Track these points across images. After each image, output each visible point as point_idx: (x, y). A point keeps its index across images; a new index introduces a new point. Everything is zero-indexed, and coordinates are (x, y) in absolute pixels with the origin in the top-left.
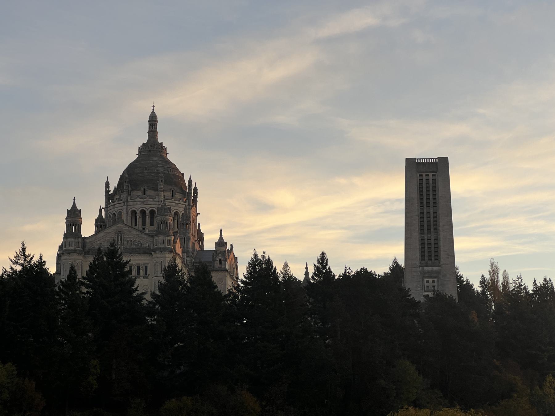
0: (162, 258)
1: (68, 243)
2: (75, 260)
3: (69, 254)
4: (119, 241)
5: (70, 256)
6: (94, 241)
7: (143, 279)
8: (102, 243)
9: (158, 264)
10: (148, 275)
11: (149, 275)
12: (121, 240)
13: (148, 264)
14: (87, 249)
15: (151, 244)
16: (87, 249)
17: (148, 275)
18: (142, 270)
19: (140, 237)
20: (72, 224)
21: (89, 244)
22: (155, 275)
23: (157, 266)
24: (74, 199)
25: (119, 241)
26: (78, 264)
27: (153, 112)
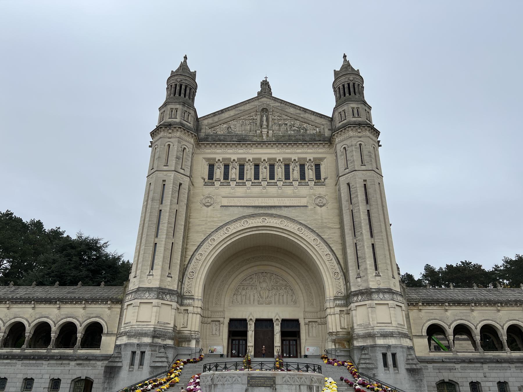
0: (360, 137)
1: (168, 113)
2: (180, 139)
3: (168, 128)
4: (265, 123)
5: (170, 131)
6: (217, 122)
7: (314, 185)
9: (354, 149)
10: (323, 180)
11: (325, 179)
12: (267, 120)
13: (322, 159)
14: (202, 135)
15: (324, 128)
16: (202, 135)
17: (323, 180)
19: (302, 117)
21: (207, 127)
25: (265, 123)
26: (185, 148)
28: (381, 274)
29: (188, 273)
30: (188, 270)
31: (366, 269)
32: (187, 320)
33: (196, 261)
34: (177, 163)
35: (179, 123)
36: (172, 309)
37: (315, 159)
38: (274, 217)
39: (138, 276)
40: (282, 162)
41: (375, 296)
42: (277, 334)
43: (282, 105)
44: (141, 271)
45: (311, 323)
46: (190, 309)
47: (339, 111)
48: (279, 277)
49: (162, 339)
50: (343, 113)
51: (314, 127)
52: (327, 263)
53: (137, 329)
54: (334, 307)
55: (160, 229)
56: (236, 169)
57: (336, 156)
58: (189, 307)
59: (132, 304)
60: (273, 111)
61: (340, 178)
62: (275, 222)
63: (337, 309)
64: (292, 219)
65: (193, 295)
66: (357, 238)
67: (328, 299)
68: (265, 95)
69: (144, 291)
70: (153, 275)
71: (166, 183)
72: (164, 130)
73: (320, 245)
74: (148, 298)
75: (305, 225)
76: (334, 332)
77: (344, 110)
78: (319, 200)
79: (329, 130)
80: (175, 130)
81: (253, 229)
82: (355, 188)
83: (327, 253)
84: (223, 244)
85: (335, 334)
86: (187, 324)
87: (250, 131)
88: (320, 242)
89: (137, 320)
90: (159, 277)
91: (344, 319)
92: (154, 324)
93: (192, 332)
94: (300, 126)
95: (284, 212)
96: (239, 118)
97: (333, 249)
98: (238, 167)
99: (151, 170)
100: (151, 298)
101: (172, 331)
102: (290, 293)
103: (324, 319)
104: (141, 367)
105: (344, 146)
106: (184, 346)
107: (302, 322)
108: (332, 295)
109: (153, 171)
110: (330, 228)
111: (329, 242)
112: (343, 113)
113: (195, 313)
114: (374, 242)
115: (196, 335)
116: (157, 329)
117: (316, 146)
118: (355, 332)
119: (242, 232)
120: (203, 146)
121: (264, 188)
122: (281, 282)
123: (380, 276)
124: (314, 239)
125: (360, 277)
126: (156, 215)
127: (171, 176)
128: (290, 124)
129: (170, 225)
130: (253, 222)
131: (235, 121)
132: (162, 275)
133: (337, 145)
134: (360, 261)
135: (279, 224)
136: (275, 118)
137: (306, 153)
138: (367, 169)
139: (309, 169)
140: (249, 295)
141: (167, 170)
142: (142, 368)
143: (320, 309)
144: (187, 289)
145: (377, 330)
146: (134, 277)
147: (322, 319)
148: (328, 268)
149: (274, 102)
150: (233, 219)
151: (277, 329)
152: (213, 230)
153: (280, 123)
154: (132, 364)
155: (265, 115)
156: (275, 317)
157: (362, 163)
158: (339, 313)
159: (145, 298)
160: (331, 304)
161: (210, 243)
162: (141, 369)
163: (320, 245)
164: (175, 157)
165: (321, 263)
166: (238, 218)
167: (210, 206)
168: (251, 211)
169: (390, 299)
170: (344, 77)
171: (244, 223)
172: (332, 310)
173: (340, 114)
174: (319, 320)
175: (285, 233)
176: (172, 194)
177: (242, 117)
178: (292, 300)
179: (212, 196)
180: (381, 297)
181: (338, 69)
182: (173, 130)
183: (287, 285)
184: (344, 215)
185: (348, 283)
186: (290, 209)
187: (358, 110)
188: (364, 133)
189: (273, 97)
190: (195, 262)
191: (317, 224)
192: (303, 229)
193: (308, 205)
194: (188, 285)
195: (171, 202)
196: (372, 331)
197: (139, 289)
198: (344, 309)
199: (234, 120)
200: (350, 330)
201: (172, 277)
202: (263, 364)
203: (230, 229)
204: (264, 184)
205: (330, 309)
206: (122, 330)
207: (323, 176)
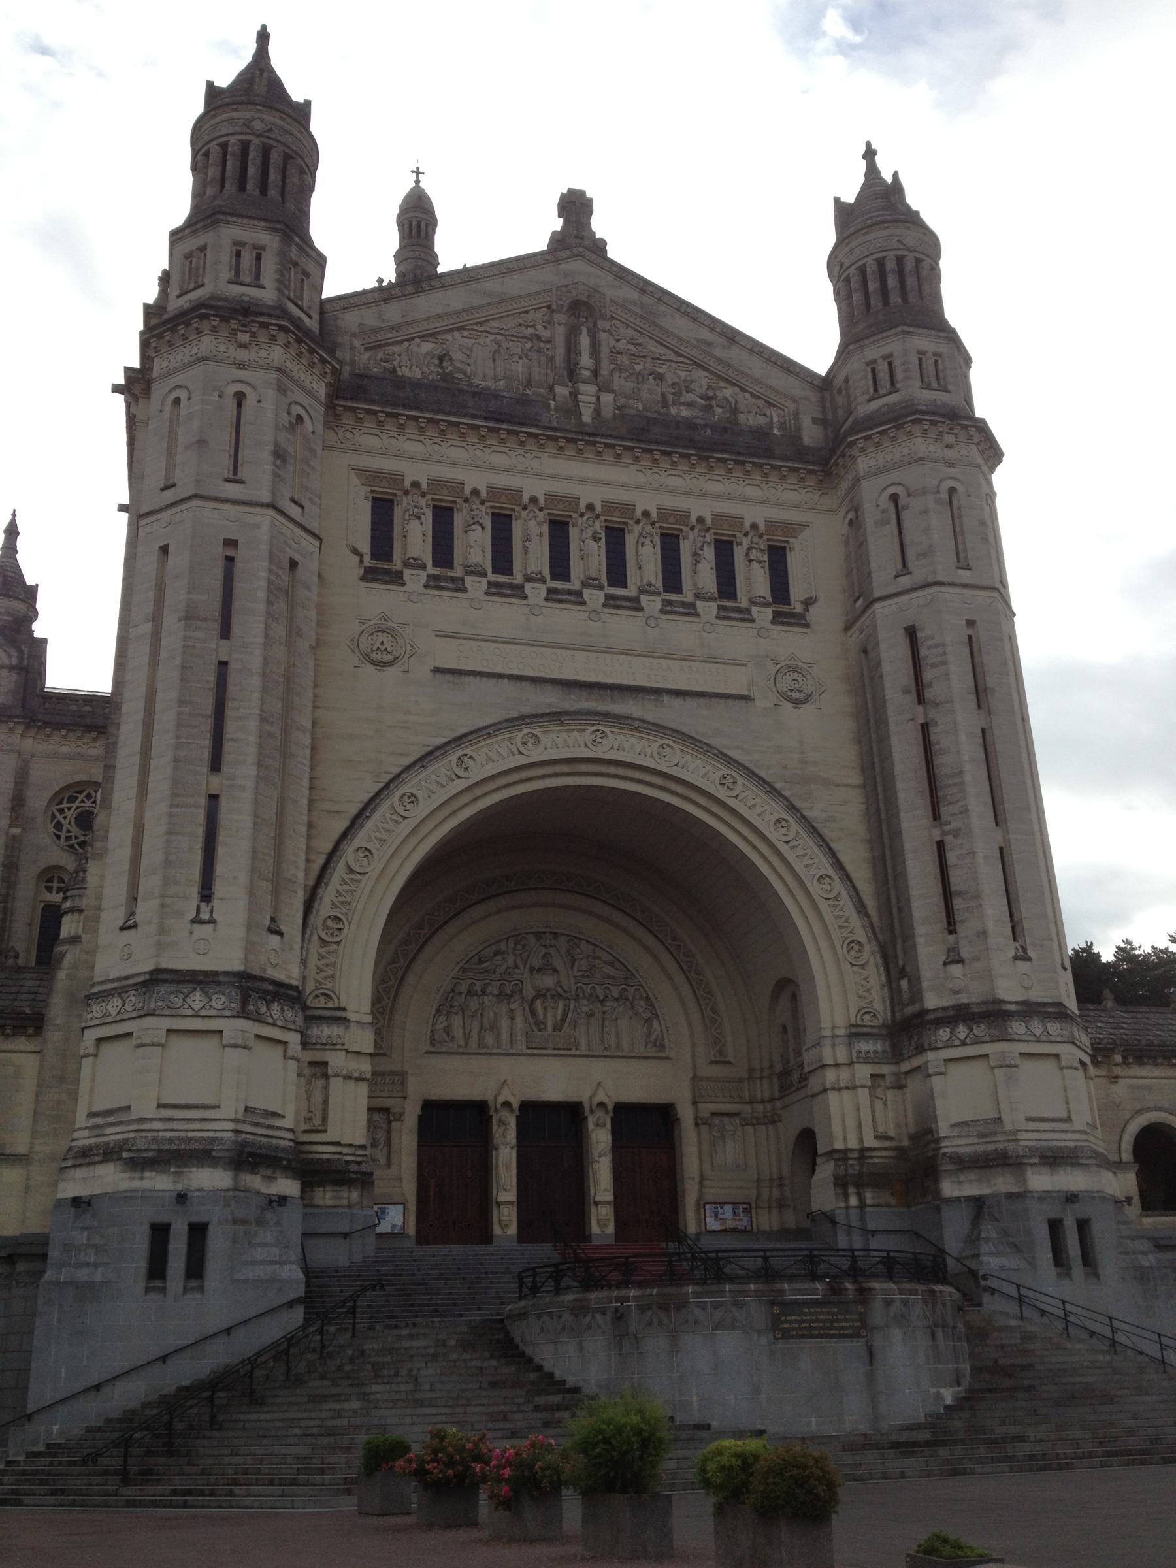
0: (951, 464)
3: (234, 325)
5: (244, 337)
8: (457, 356)
11: (808, 603)
13: (793, 529)
18: (754, 564)
19: (719, 360)
22: (905, 581)
23: (926, 512)
25: (586, 360)
28: (1031, 953)
29: (319, 924)
30: (318, 911)
31: (983, 934)
32: (325, 1102)
33: (346, 877)
34: (279, 476)
35: (272, 307)
36: (285, 1057)
37: (772, 525)
38: (637, 729)
40: (653, 524)
41: (1017, 1027)
42: (603, 1159)
43: (646, 299)
44: (163, 906)
45: (717, 1121)
46: (336, 1061)
47: (870, 358)
48: (599, 953)
49: (264, 1177)
50: (883, 368)
51: (761, 403)
52: (823, 906)
53: (162, 1134)
54: (851, 1064)
55: (232, 739)
56: (483, 528)
57: (855, 524)
58: (328, 1052)
59: (131, 1034)
60: (612, 316)
61: (877, 606)
62: (638, 748)
63: (863, 1072)
64: (701, 742)
65: (342, 1005)
66: (949, 823)
67: (827, 1033)
68: (581, 249)
69: (178, 982)
70: (212, 921)
71: (241, 554)
72: (214, 330)
73: (797, 843)
74: (203, 1013)
75: (745, 767)
76: (851, 1150)
77: (890, 355)
78: (789, 678)
79: (815, 420)
80: (263, 336)
81: (559, 769)
82: (937, 646)
83: (823, 872)
84: (445, 819)
85: (856, 1155)
86: (325, 1119)
87: (529, 384)
88: (798, 833)
89: (159, 1099)
90: (241, 933)
91: (885, 1104)
92: (232, 1116)
93: (345, 1150)
94: (711, 393)
95: (671, 713)
96: (482, 323)
97: (843, 858)
98: (487, 522)
99: (163, 490)
100: (212, 1013)
101: (292, 1144)
102: (641, 1010)
103: (768, 1106)
104: (194, 1283)
105: (892, 490)
106: (321, 1203)
107: (686, 1114)
108: (840, 1021)
109: (170, 496)
110: (827, 782)
111: (825, 832)
112: (883, 368)
113: (350, 1078)
114: (1007, 840)
115: (359, 1159)
116: (244, 1136)
117: (774, 478)
118: (943, 1151)
119: (516, 777)
120: (348, 420)
121: (593, 616)
122: (608, 970)
123: (1029, 959)
124: (778, 821)
125: (961, 961)
126: (207, 682)
127: (257, 526)
128: (676, 380)
129: (267, 728)
130: (559, 741)
131: (466, 333)
132: (249, 928)
133: (865, 484)
134: (958, 903)
135: (652, 756)
136: (618, 345)
137: (741, 499)
138: (978, 583)
139: (750, 561)
140: (492, 1014)
141: (244, 498)
142: (201, 1289)
143: (751, 1070)
144: (317, 981)
145: (1027, 1140)
146: (123, 929)
147: (760, 1107)
148: (825, 925)
149: (616, 283)
150: (481, 725)
151: (600, 1138)
152: (407, 761)
153: (638, 368)
154: (157, 1269)
155: (584, 330)
156: (595, 1094)
157: (959, 561)
158: (869, 1084)
159: (190, 1012)
160: (838, 1053)
161: (400, 810)
162: (198, 1296)
163: (797, 843)
164: (270, 448)
165: (799, 906)
166: (499, 723)
167: (391, 663)
168: (549, 699)
169: (1066, 1040)
170: (886, 233)
171: (524, 743)
172: (844, 1075)
173: (869, 369)
174: (748, 1108)
176: (269, 603)
177: (495, 324)
178: (648, 1036)
179: (395, 626)
180: (1038, 1032)
181: (849, 197)
182: (253, 335)
183: (630, 982)
184: (894, 740)
185: (904, 983)
186: (690, 703)
187: (936, 362)
188: (964, 452)
189: (613, 263)
190: (343, 880)
191: (785, 767)
192: (740, 780)
194: (318, 968)
195: (266, 636)
196: (1010, 1147)
197: (157, 979)
198: (886, 1069)
199: (458, 329)
200: (906, 1143)
201: (281, 934)
202: (723, 1258)
203: (471, 761)
204: (593, 597)
205: (833, 1068)
206: (84, 1139)
207: (797, 592)
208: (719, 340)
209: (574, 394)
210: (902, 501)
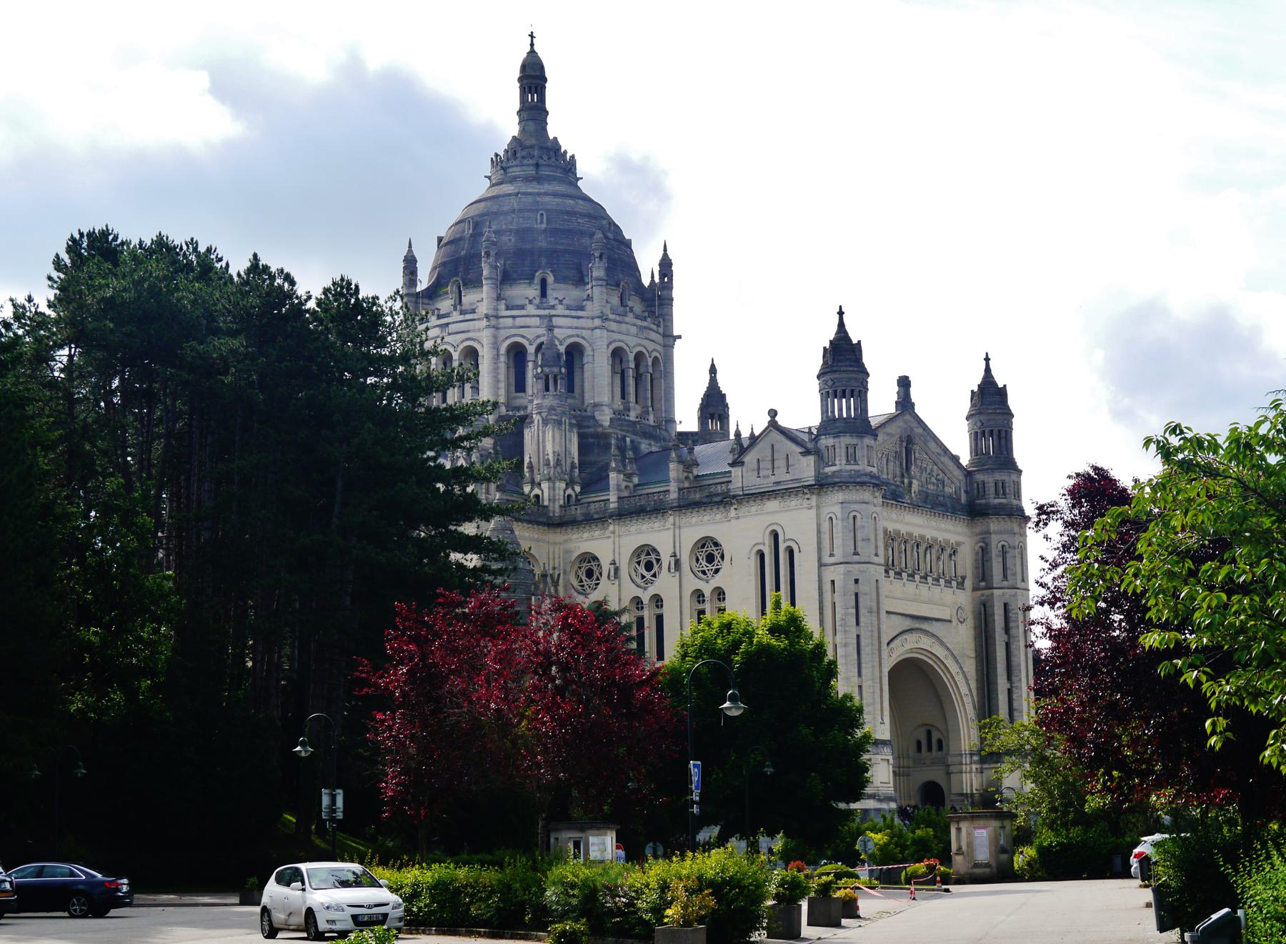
19: (942, 463)
20: (839, 390)
23: (1015, 557)
24: (841, 313)
27: (532, 52)
39: (870, 722)
63: (974, 767)
105: (1003, 543)
134: (1016, 714)
147: (902, 769)
168: (908, 624)
175: (932, 659)
186: (939, 624)
193: (953, 620)
208: (942, 453)
209: (910, 483)
210: (1007, 548)
